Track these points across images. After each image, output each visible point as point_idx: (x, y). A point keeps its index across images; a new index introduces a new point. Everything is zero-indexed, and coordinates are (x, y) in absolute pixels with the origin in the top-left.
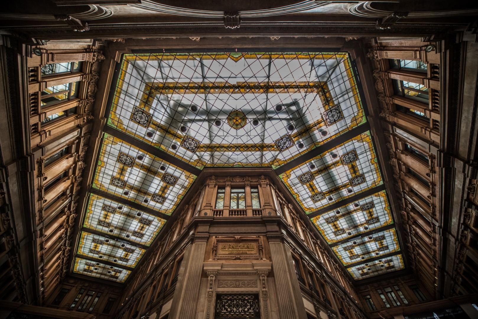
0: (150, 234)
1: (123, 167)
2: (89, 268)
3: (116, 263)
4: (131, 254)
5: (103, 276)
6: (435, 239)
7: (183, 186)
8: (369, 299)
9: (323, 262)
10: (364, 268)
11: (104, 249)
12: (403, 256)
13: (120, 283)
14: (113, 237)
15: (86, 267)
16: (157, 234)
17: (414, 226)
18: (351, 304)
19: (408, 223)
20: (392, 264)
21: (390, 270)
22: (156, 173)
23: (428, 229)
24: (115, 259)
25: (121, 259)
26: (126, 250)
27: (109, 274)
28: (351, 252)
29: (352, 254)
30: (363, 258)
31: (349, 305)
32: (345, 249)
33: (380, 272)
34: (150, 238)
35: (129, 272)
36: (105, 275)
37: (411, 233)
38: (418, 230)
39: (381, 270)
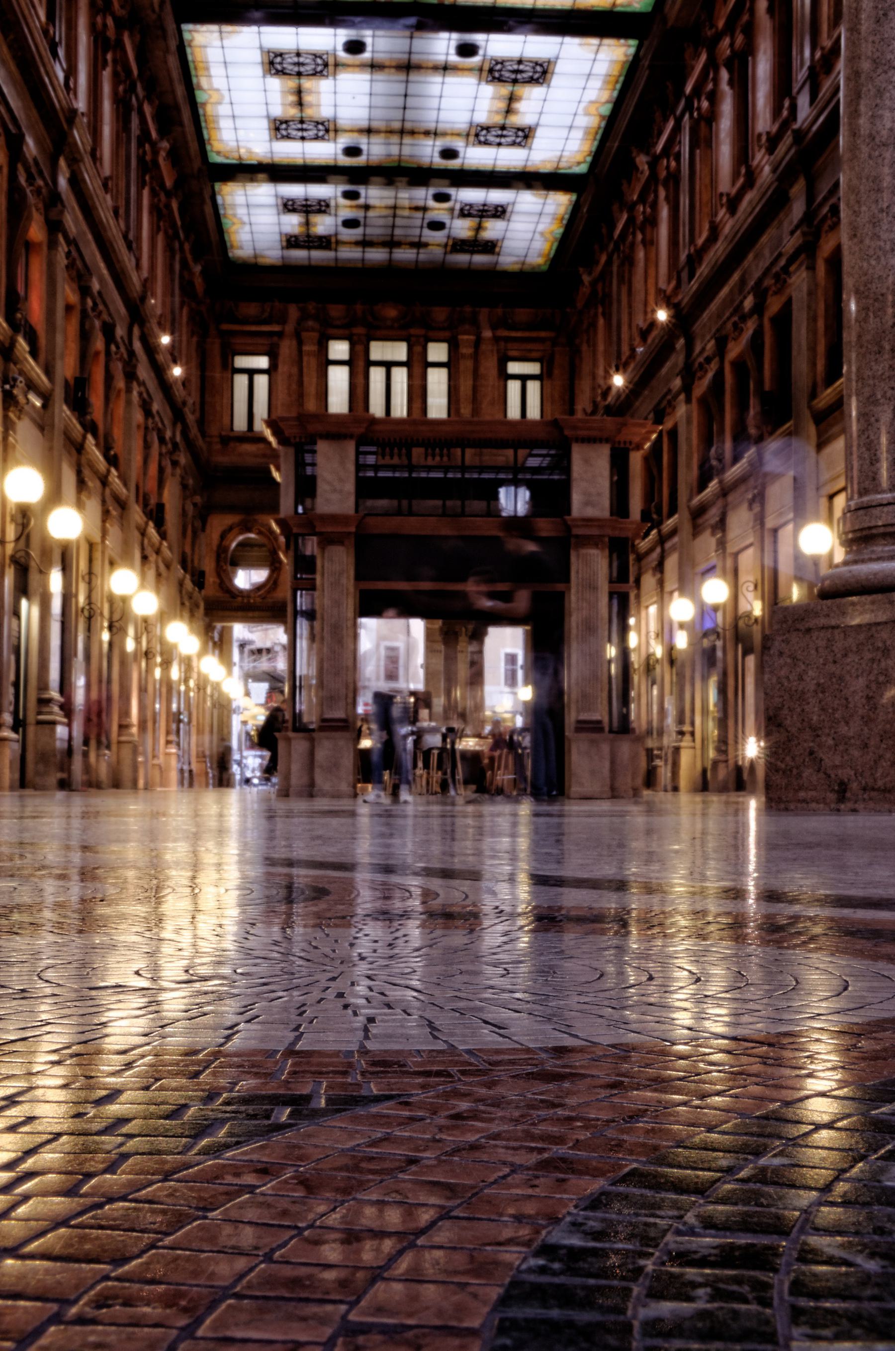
6: (750, 180)
8: (251, 373)
9: (81, 104)
10: (322, 207)
12: (576, 209)
17: (724, 75)
18: (144, 372)
19: (712, 45)
20: (493, 229)
21: (462, 258)
23: (763, 121)
28: (299, 92)
29: (300, 104)
30: (352, 151)
31: (131, 376)
32: (275, 63)
33: (405, 255)
37: (689, 107)
38: (727, 108)
39: (419, 245)
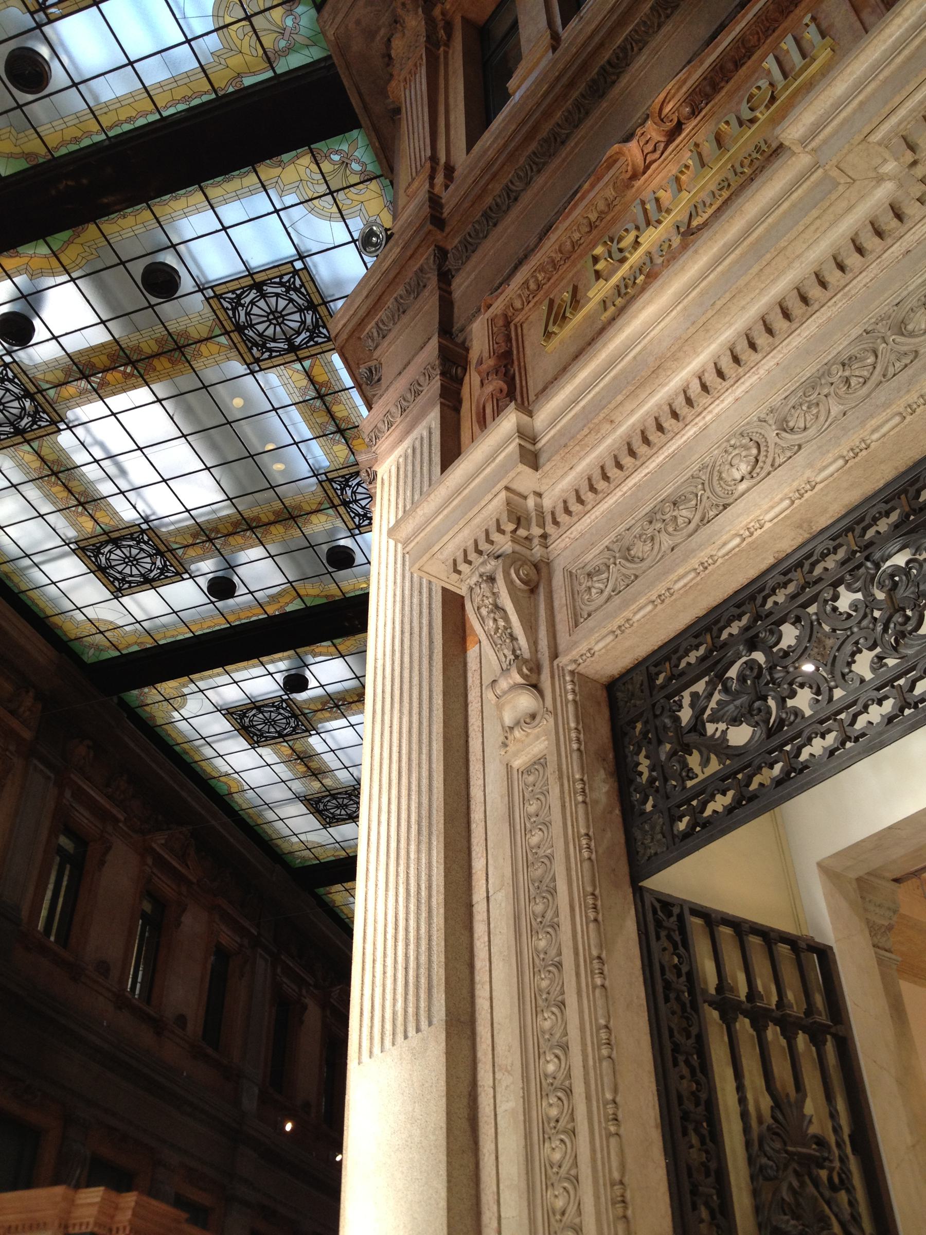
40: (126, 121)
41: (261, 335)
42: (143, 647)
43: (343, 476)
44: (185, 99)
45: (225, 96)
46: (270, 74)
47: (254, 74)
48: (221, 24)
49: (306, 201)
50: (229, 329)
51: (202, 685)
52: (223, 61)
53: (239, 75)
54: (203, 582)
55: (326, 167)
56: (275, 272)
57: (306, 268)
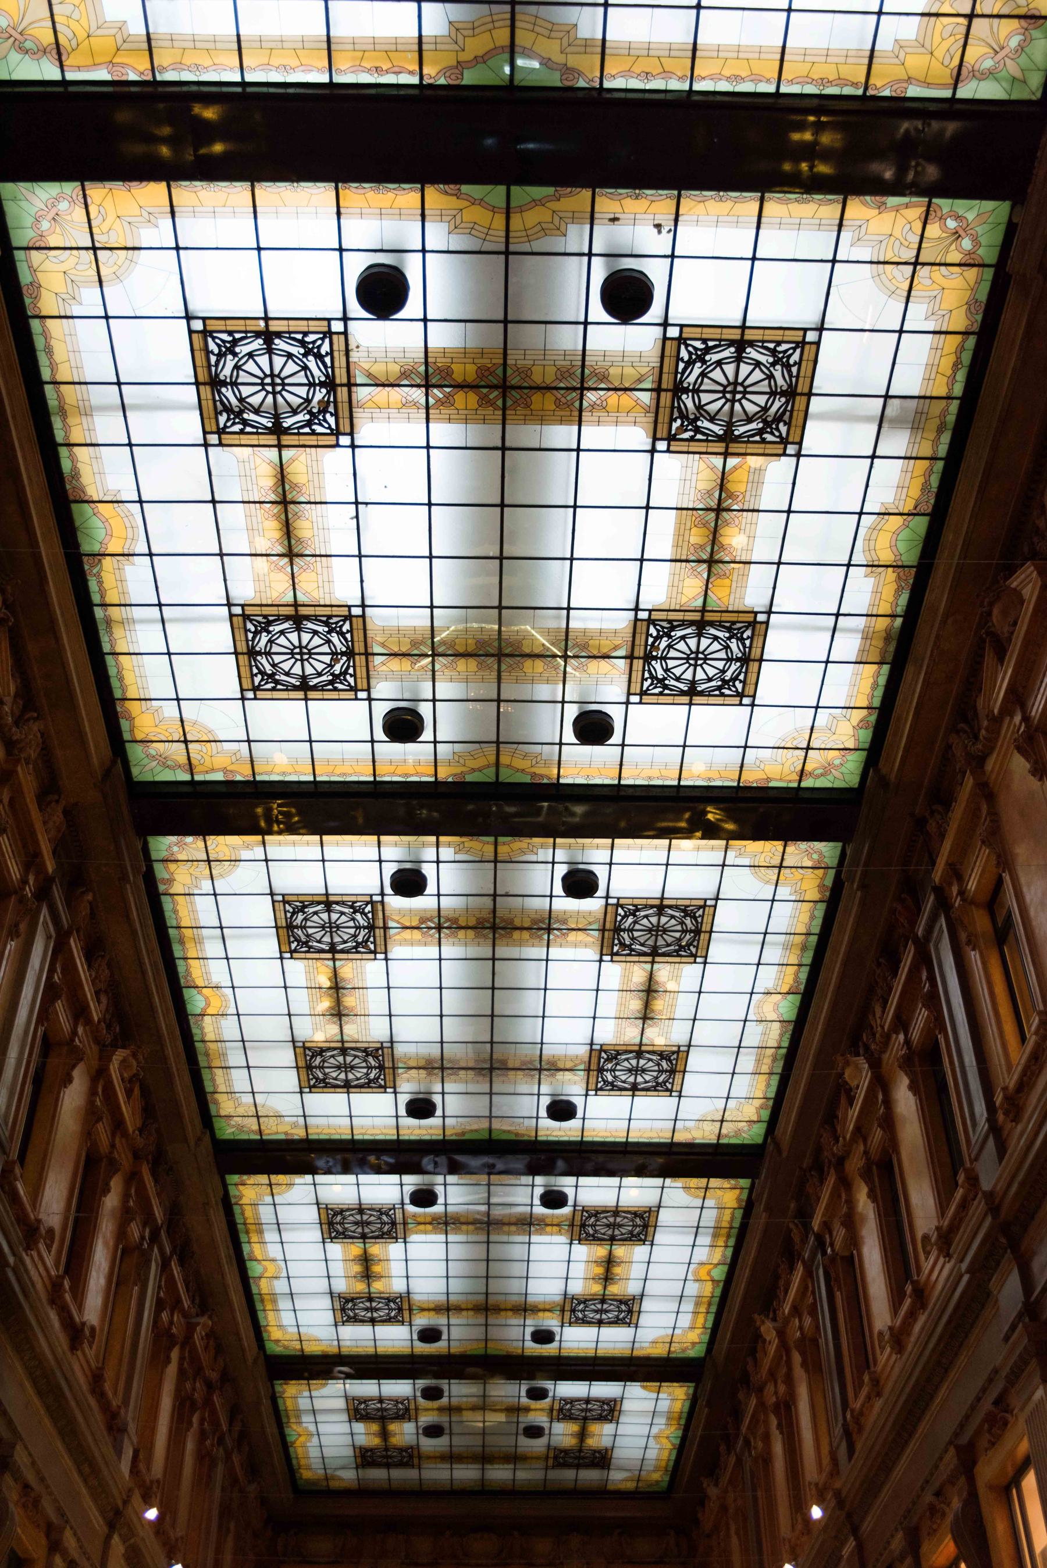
0: (728, 1026)
1: (282, 476)
2: (384, 1434)
3: (549, 1349)
4: (640, 1252)
5: (499, 1474)
7: (890, 409)
11: (423, 1265)
13: (640, 1495)
14: (454, 1154)
15: (365, 1434)
16: (786, 1007)
22: (576, 389)
24: (531, 1324)
25: (574, 1310)
26: (588, 1226)
27: (538, 1445)
34: (747, 1062)
35: (674, 1397)
36: (514, 1458)
40: (728, 79)
41: (699, 407)
42: (230, 778)
43: (670, 622)
44: (823, 81)
45: (874, 98)
46: (947, 94)
47: (929, 85)
48: (933, 11)
49: (879, 263)
50: (664, 386)
51: (273, 852)
52: (902, 55)
53: (909, 80)
54: (381, 710)
55: (933, 230)
56: (778, 335)
57: (818, 344)
